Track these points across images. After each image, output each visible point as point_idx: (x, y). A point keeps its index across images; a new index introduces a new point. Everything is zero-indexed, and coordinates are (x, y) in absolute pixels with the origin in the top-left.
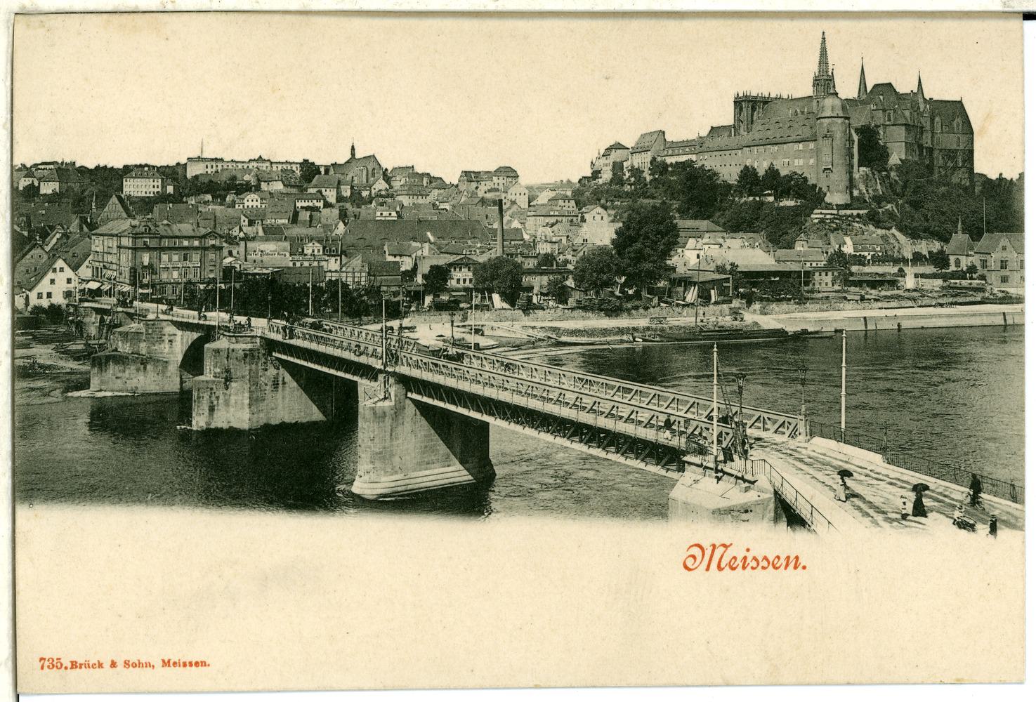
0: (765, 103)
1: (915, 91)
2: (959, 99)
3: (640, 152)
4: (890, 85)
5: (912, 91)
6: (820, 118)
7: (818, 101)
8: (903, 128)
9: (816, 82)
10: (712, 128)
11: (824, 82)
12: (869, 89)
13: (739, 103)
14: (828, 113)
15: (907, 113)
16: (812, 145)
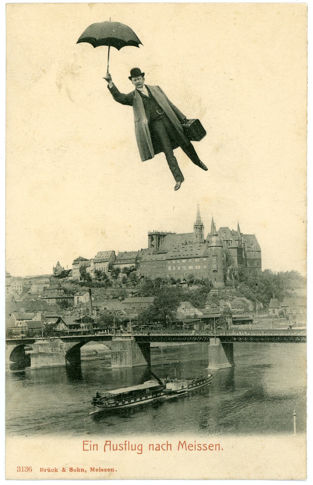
0: (165, 236)
1: (236, 229)
2: (254, 234)
3: (101, 262)
4: (227, 228)
5: (233, 230)
6: (210, 247)
7: (197, 236)
8: (236, 249)
9: (196, 227)
10: (142, 250)
11: (199, 227)
12: (217, 230)
13: (151, 236)
14: (215, 245)
15: (237, 242)
16: (205, 259)
